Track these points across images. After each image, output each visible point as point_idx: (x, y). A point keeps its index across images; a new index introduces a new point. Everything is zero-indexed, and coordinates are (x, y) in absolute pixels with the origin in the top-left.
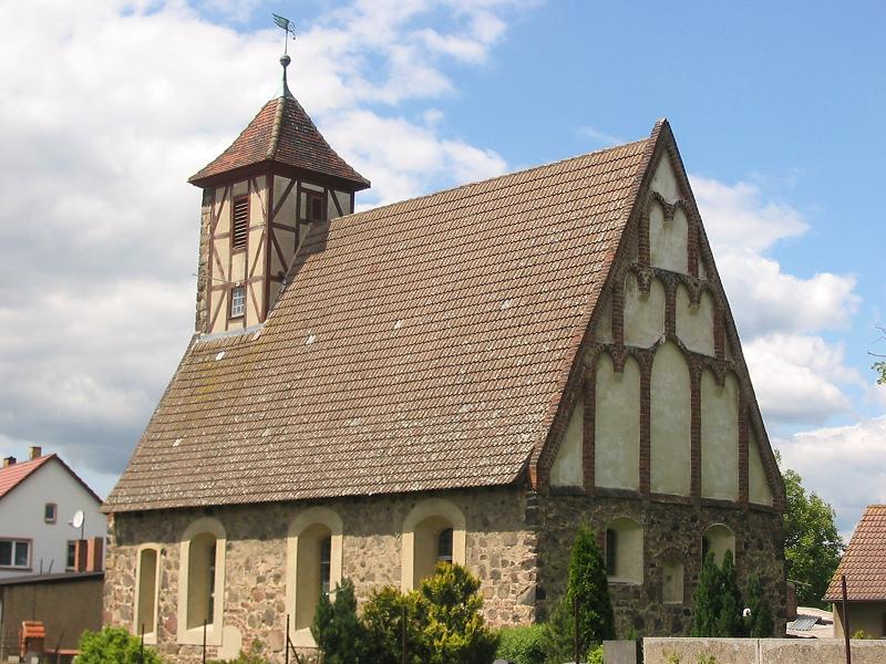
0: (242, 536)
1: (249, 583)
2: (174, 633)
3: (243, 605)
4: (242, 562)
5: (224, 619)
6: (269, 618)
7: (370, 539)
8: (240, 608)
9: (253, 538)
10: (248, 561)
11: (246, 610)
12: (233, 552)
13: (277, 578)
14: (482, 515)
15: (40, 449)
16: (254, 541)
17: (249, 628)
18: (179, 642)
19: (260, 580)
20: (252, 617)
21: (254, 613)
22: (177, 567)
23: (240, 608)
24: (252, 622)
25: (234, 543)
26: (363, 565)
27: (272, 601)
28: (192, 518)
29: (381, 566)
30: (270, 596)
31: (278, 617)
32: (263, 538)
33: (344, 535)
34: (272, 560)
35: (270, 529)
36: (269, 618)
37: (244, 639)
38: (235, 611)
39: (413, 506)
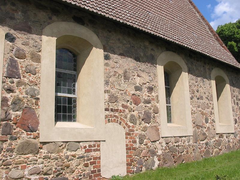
0: (119, 53)
1: (129, 89)
2: (32, 130)
3: (123, 106)
4: (121, 72)
5: (106, 117)
6: (147, 118)
7: (199, 79)
8: (121, 108)
9: (128, 57)
10: (125, 72)
11: (127, 111)
12: (110, 62)
13: (151, 89)
14: (232, 80)
15: (168, 122)
16: (130, 59)
17: (131, 125)
18: (42, 139)
19: (137, 89)
20: (132, 116)
21: (135, 113)
22: (37, 59)
23: (121, 108)
24: (133, 120)
25: (111, 55)
26: (198, 91)
27: (149, 105)
28: (54, 18)
29: (205, 93)
30: (148, 102)
31: (154, 117)
32: (137, 59)
33: (189, 73)
34: (146, 78)
35: (142, 54)
36: (147, 118)
37: (127, 134)
38: (117, 110)
39: (212, 69)
